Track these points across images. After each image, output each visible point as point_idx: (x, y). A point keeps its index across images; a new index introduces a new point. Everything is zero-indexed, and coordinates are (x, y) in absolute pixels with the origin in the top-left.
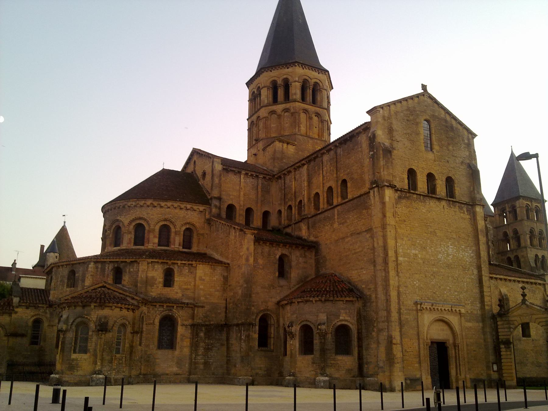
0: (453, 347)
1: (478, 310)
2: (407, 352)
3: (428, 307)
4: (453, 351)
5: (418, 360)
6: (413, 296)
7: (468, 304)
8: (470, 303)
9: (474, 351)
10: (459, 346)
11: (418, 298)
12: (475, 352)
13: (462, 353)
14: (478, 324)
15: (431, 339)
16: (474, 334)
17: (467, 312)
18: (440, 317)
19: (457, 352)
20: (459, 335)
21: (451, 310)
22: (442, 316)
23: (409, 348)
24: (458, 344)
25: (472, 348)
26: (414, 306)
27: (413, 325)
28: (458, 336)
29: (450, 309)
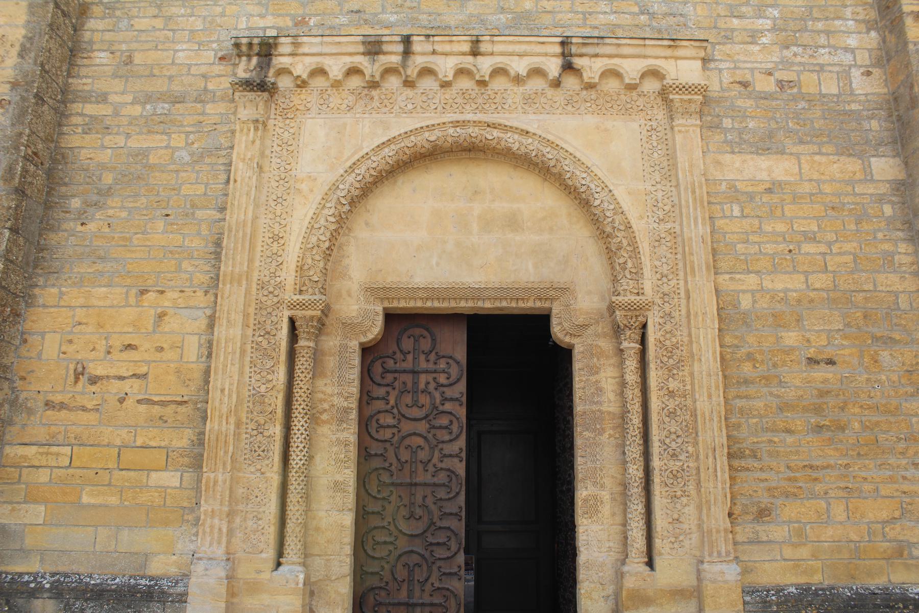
0: (606, 345)
1: (856, 73)
2: (94, 380)
3: (336, 68)
4: (607, 378)
5: (182, 440)
6: (223, 15)
7: (753, 36)
8: (774, 29)
9: (812, 361)
10: (644, 326)
11: (270, 21)
12: (821, 373)
13: (673, 385)
14: (852, 166)
15: (374, 291)
16: (811, 238)
17: (745, 85)
18: (456, 124)
19: (632, 377)
20: (645, 247)
21: (568, 67)
22: (480, 117)
23: (116, 355)
24: (641, 309)
25: (791, 338)
26: (218, 69)
27: (186, 190)
28: (635, 251)
29: (553, 67)
